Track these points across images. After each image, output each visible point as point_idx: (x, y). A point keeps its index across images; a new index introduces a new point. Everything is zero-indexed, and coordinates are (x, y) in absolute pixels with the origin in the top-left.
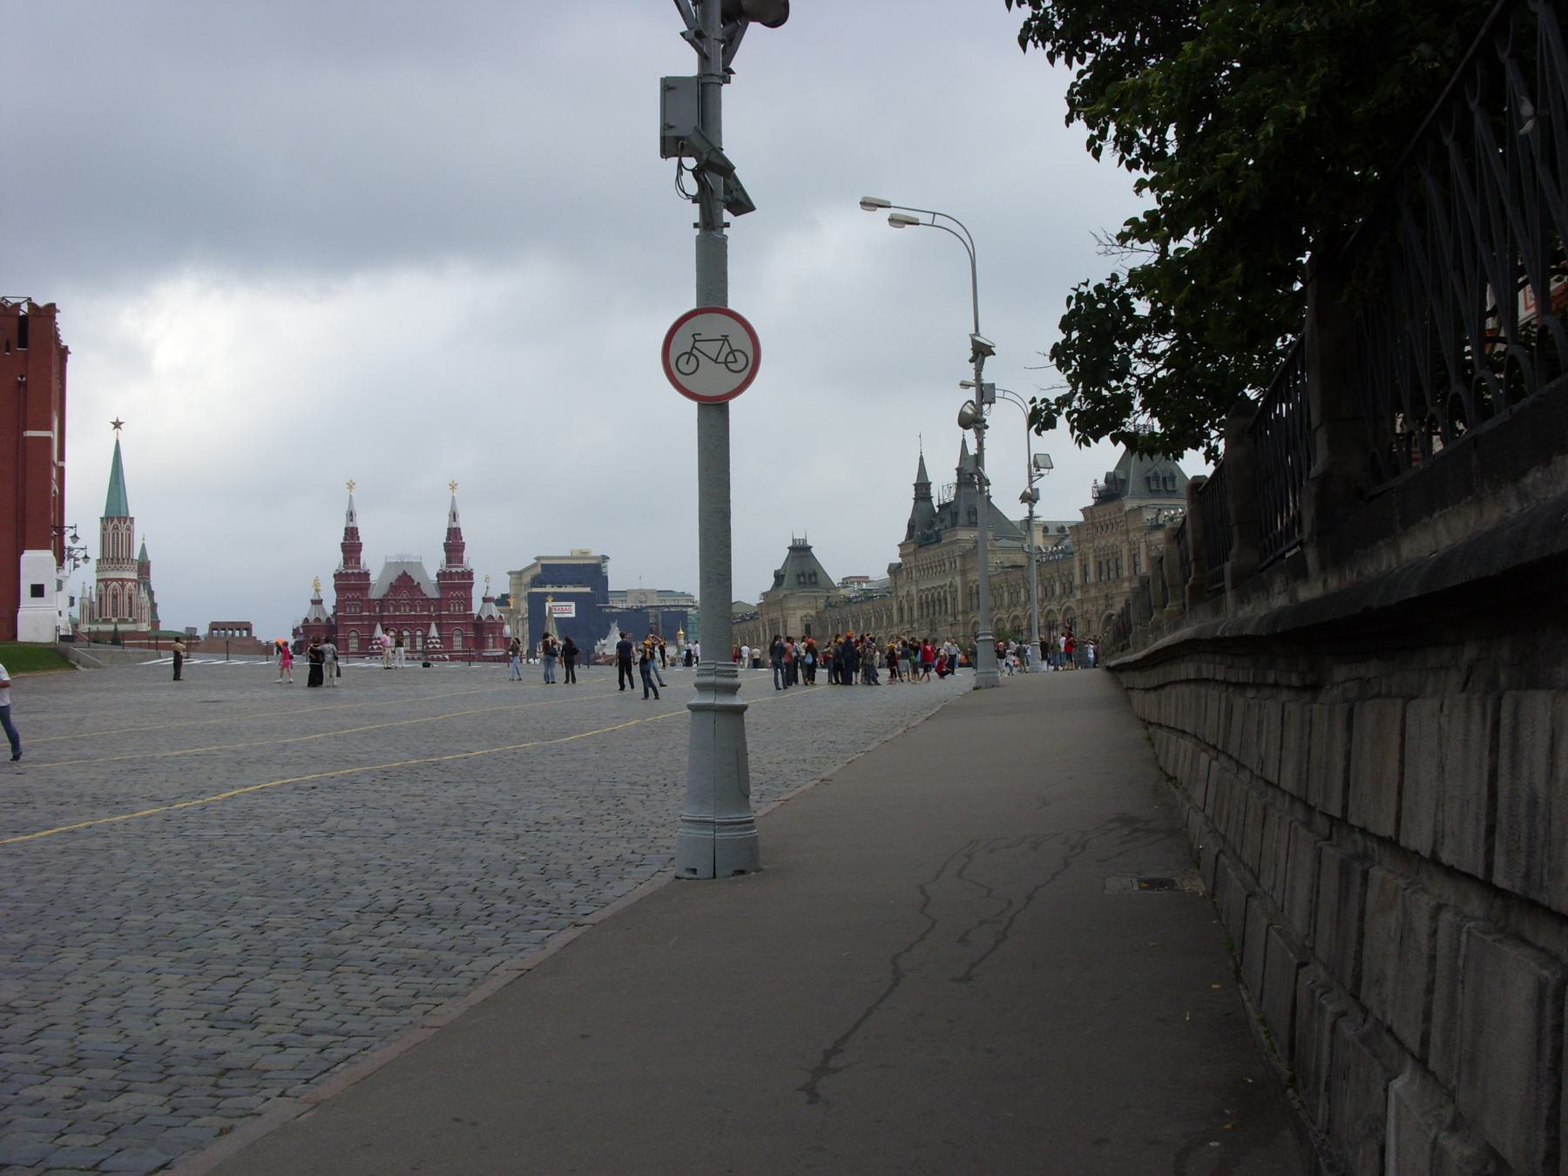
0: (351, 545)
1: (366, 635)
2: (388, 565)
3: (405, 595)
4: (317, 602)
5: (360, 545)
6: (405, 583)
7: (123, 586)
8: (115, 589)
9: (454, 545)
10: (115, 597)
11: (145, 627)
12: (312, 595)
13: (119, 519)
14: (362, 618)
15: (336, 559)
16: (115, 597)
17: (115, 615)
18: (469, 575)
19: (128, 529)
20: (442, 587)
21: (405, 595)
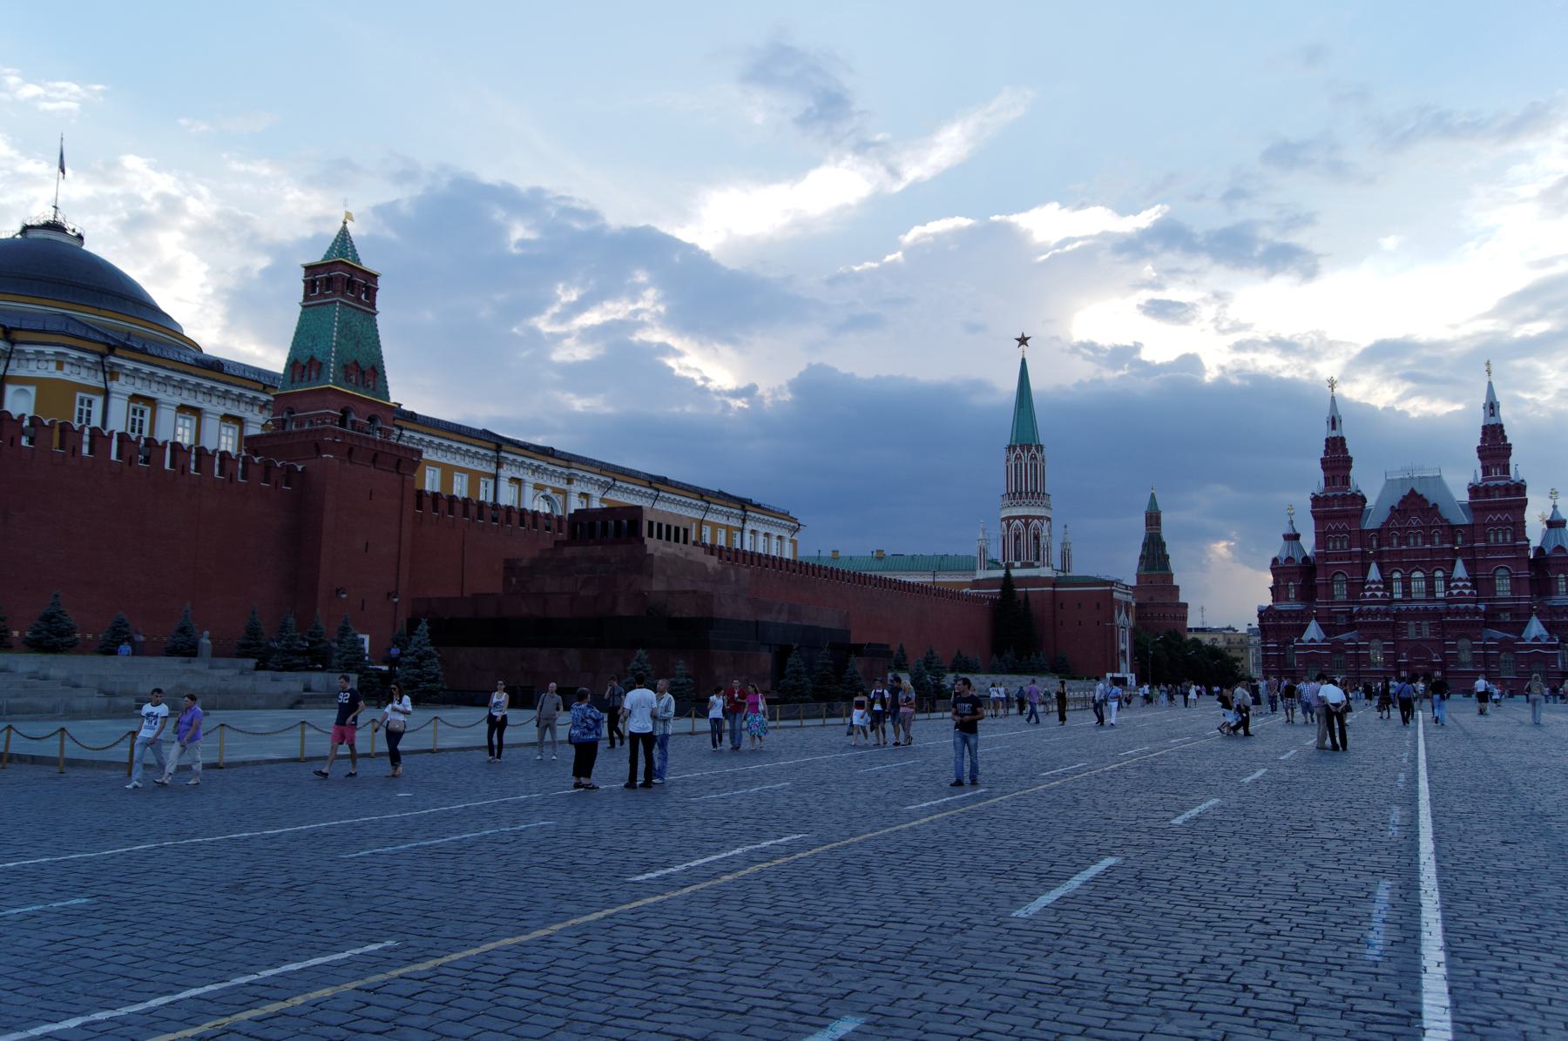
0: (1336, 458)
1: (1358, 578)
2: (1390, 483)
3: (1415, 521)
4: (1293, 537)
5: (1349, 460)
6: (1415, 506)
7: (1027, 525)
8: (1017, 528)
9: (1494, 445)
10: (1017, 537)
11: (1045, 572)
12: (1287, 530)
13: (1022, 447)
14: (1351, 556)
15: (1316, 480)
16: (1017, 537)
17: (1017, 558)
18: (1520, 488)
19: (1034, 458)
20: (1473, 508)
21: (1415, 521)
